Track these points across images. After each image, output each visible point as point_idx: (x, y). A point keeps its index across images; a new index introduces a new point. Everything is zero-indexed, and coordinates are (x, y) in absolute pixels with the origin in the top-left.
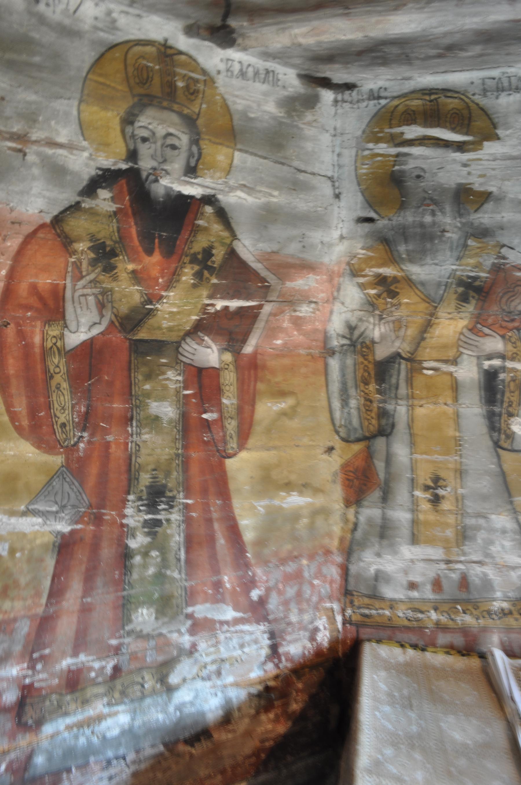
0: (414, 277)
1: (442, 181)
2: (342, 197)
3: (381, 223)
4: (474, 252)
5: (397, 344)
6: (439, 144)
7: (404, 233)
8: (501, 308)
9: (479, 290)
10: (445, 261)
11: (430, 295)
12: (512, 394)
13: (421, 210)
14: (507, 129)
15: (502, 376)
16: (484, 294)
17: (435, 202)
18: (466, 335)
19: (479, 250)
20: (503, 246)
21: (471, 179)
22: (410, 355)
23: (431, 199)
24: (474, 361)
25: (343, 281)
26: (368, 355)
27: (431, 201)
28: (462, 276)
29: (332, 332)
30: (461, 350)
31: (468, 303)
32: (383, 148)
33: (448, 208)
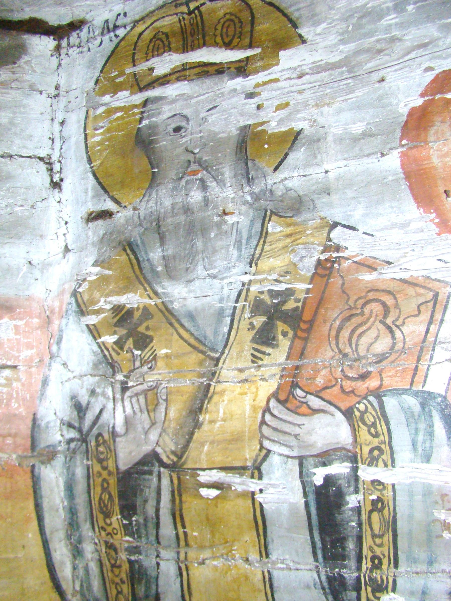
0: (176, 305)
1: (216, 129)
2: (64, 185)
3: (122, 216)
4: (281, 244)
5: (153, 436)
6: (208, 72)
7: (158, 228)
8: (340, 351)
9: (294, 319)
10: (228, 269)
11: (205, 337)
12: (378, 541)
13: (183, 182)
14: (317, 24)
15: (352, 500)
16: (303, 326)
17: (205, 166)
18: (275, 412)
19: (289, 240)
20: (336, 225)
21: (263, 116)
22: (175, 459)
23: (199, 162)
24: (294, 465)
25: (67, 324)
26: (107, 459)
27: (198, 166)
28: (262, 293)
29: (51, 417)
30: (267, 444)
31: (274, 346)
32: (124, 98)
33: (227, 173)
